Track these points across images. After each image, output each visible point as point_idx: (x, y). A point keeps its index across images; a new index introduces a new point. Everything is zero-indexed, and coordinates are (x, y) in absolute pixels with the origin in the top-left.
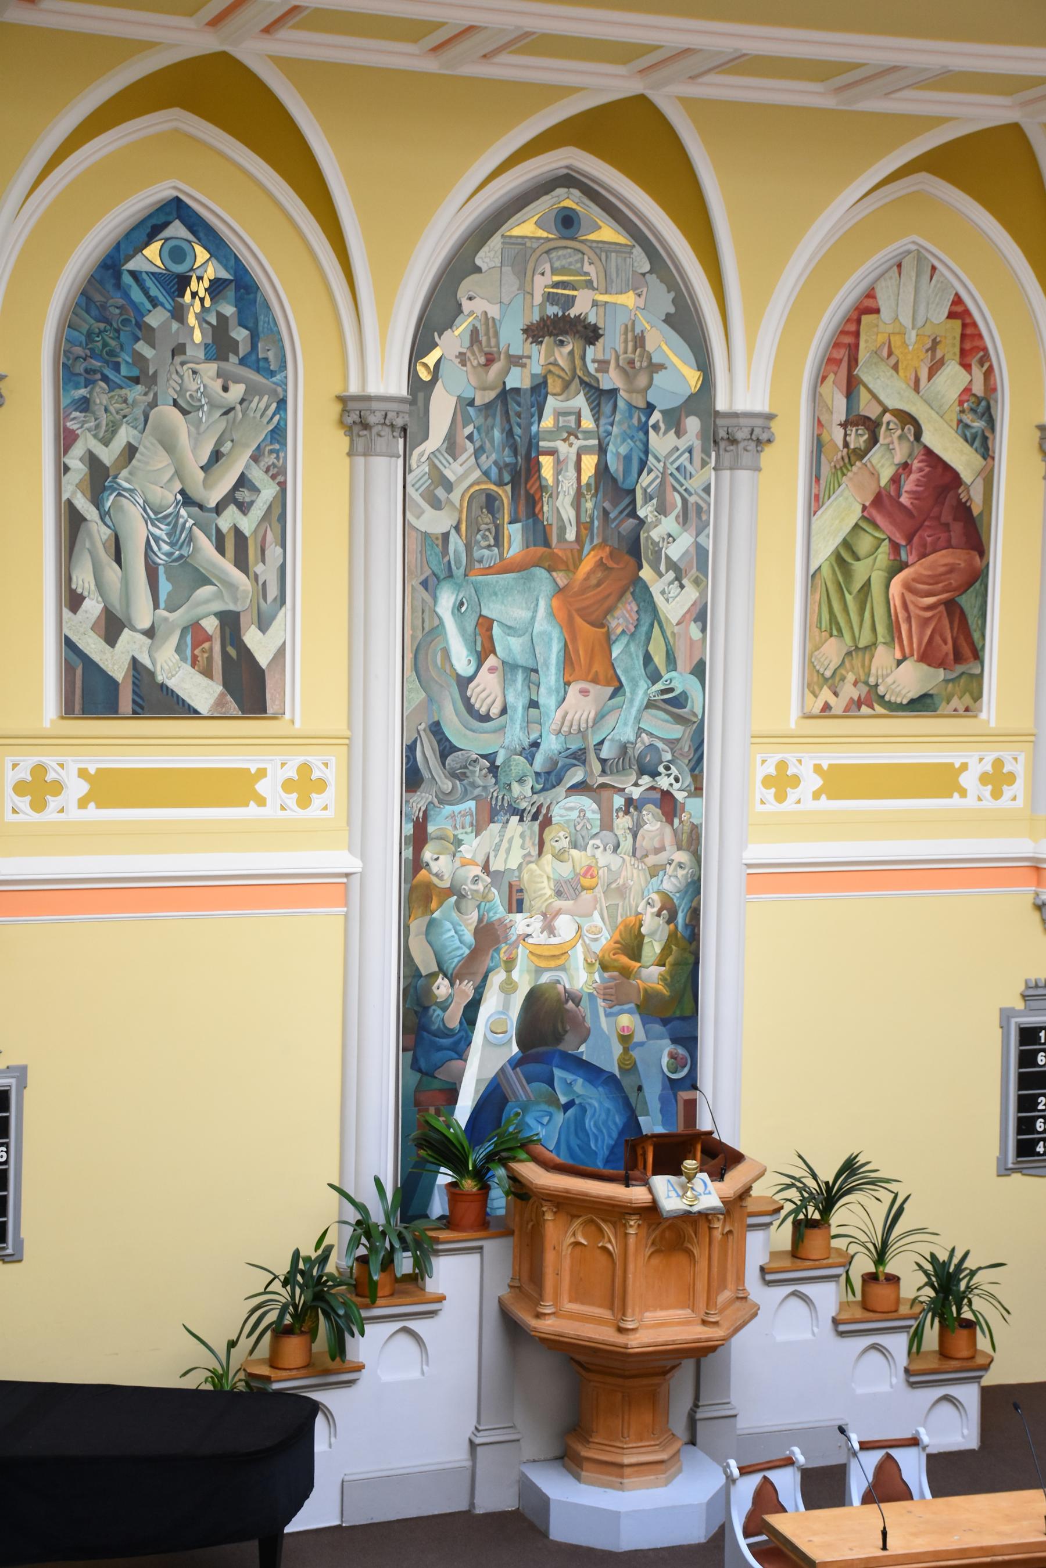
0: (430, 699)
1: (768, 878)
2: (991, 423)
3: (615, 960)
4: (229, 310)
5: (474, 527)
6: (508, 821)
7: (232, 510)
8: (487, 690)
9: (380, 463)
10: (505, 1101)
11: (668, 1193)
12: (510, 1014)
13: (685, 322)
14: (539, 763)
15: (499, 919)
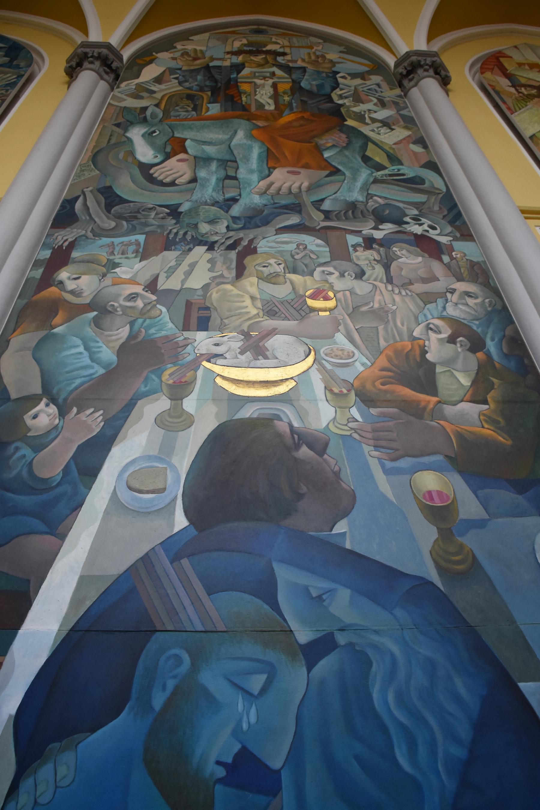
3: (386, 392)
6: (190, 250)
10: (144, 631)
12: (175, 460)
15: (167, 337)
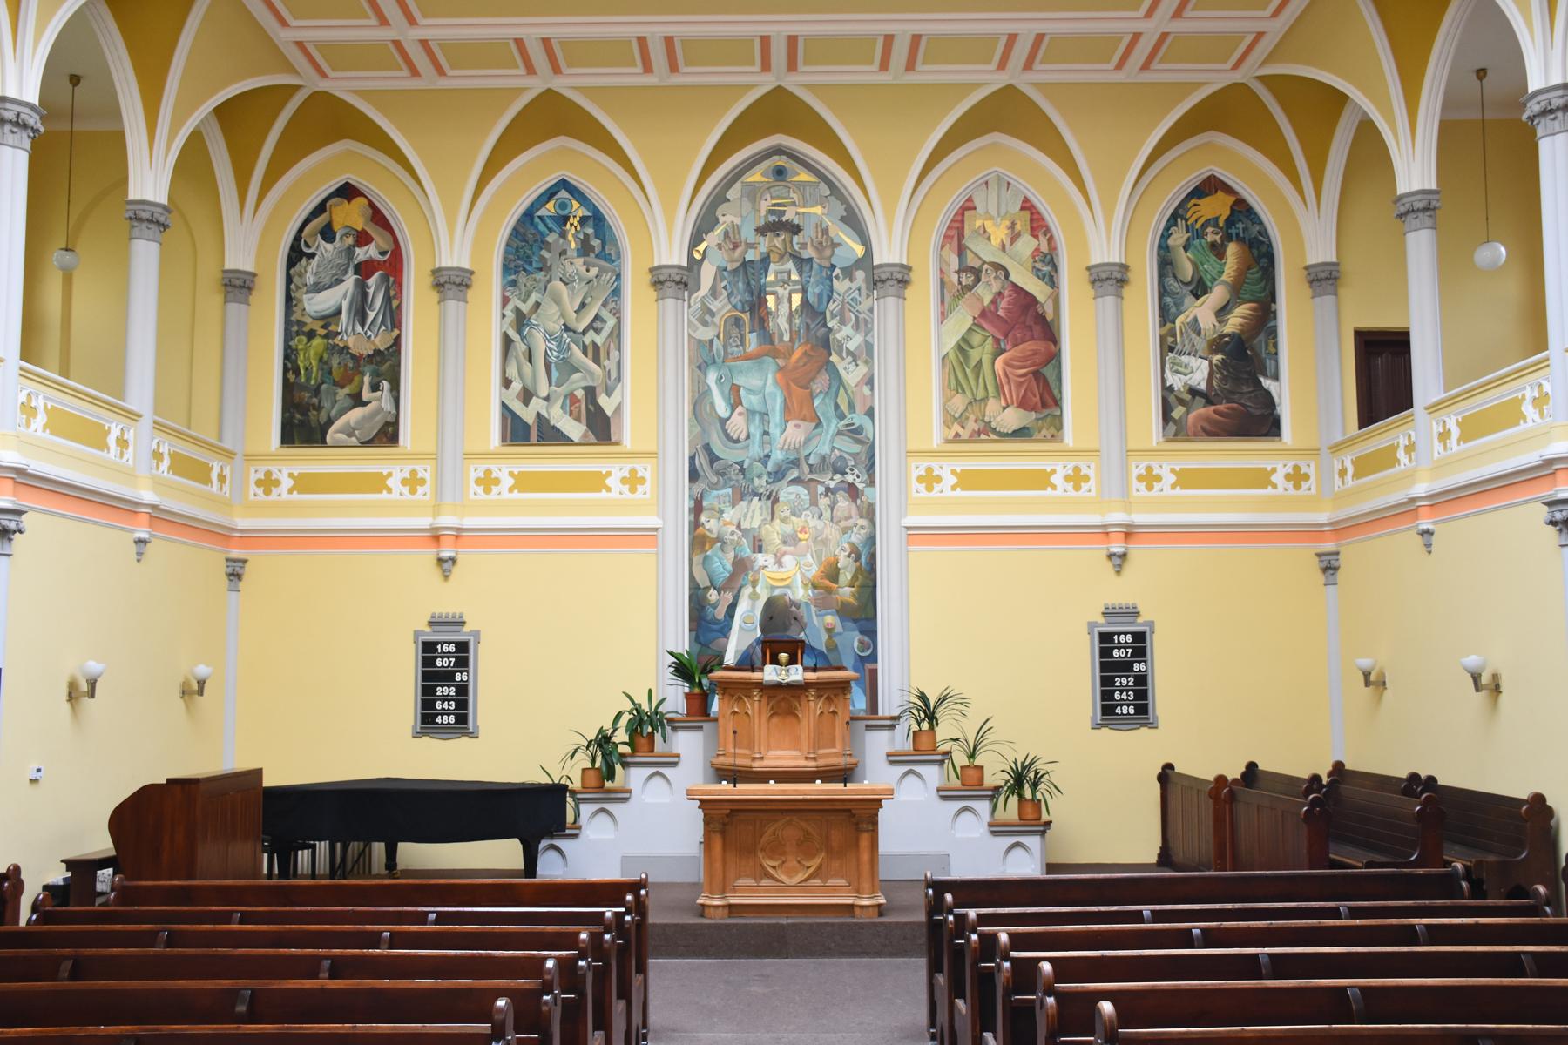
0: (704, 430)
1: (916, 535)
2: (1055, 268)
4: (590, 231)
5: (728, 336)
7: (591, 332)
8: (737, 425)
9: (670, 302)
11: (770, 674)
13: (852, 220)
14: (770, 467)
